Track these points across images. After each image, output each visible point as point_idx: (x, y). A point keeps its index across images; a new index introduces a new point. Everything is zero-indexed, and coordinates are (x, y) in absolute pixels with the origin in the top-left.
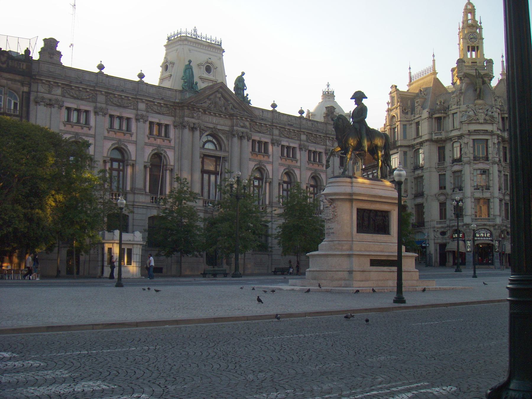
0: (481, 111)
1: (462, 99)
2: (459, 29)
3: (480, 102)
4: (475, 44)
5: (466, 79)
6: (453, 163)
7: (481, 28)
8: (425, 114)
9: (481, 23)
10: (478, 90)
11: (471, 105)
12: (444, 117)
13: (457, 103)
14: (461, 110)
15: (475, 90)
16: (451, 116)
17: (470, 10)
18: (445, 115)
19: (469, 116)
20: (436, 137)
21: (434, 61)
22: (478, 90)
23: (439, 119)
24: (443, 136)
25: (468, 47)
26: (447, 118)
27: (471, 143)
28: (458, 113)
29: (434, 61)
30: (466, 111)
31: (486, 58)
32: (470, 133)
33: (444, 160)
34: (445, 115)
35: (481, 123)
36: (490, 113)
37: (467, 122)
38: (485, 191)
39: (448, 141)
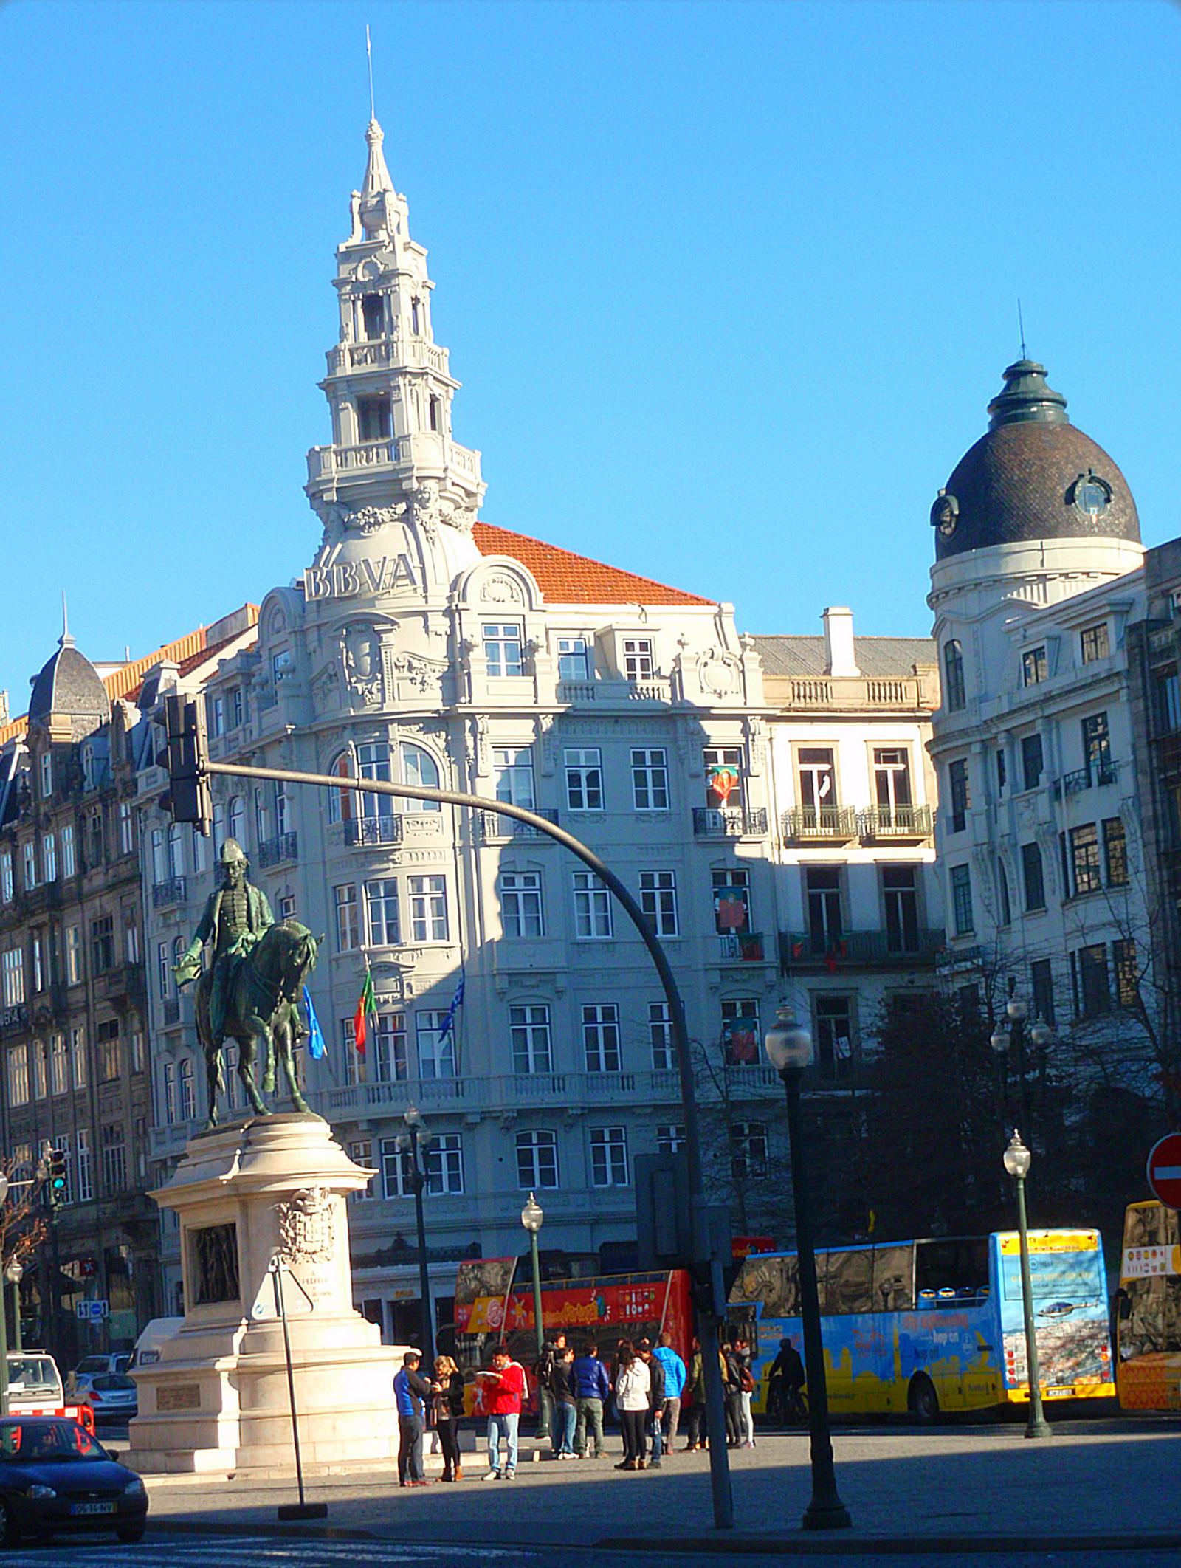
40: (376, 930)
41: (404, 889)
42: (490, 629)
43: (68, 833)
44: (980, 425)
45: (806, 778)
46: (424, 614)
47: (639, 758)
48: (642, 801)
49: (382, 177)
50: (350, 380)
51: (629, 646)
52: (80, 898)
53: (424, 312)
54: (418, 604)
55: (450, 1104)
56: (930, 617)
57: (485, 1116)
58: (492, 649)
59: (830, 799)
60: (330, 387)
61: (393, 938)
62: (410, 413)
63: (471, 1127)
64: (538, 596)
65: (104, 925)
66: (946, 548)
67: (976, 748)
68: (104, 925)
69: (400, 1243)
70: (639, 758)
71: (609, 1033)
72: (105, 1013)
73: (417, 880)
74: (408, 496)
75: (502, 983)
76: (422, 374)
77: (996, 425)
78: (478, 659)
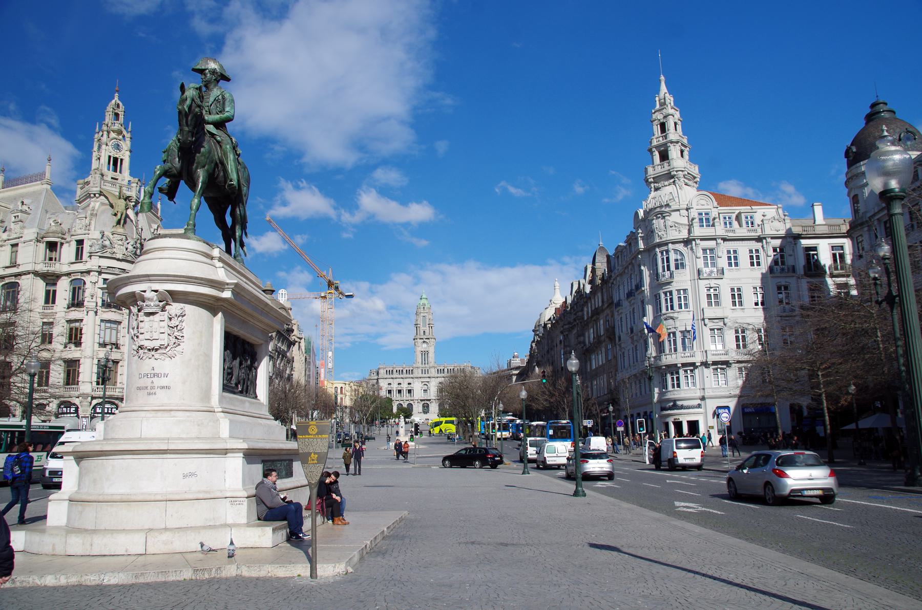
0: (120, 242)
1: (93, 222)
3: (120, 230)
6: (68, 308)
8: (30, 233)
12: (62, 244)
14: (90, 236)
16: (74, 244)
19: (104, 247)
20: (46, 269)
23: (52, 246)
24: (57, 268)
25: (110, 157)
26: (65, 246)
27: (101, 284)
33: (54, 302)
35: (118, 260)
37: (99, 254)
38: (114, 350)
39: (63, 278)
40: (667, 307)
41: (675, 294)
43: (600, 295)
46: (678, 210)
47: (751, 251)
48: (752, 264)
49: (663, 88)
50: (656, 147)
51: (747, 218)
52: (603, 311)
53: (679, 127)
54: (677, 207)
58: (701, 220)
61: (672, 308)
62: (674, 152)
63: (696, 367)
64: (716, 204)
67: (866, 229)
71: (744, 337)
73: (679, 291)
74: (673, 177)
76: (677, 142)
77: (866, 124)
78: (696, 223)
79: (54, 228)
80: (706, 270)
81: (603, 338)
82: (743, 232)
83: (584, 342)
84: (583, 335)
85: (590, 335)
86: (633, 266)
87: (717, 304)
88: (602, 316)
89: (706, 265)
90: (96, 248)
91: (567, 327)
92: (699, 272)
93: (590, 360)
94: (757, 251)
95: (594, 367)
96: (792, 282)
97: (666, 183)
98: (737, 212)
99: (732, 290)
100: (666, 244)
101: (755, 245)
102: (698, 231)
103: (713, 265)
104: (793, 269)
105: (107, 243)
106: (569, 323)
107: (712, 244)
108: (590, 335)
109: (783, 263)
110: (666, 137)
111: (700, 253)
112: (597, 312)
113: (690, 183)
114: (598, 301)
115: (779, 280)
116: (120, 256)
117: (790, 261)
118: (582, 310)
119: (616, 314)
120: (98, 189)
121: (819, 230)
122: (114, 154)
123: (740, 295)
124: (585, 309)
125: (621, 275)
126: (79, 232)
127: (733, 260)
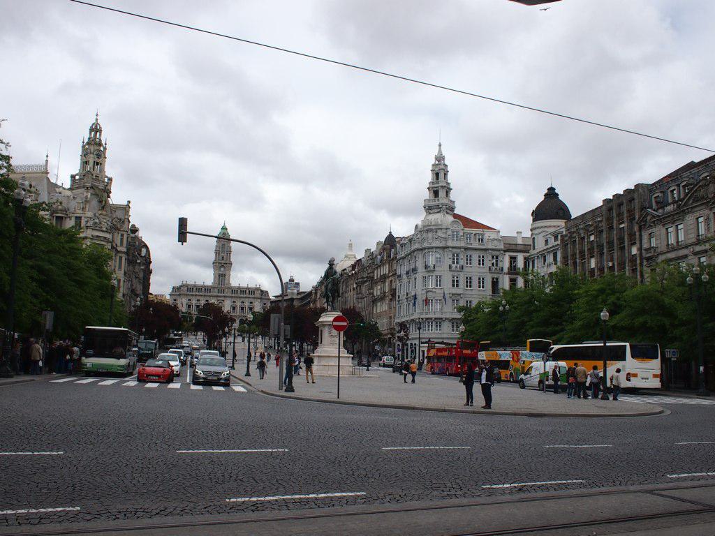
1: (87, 206)
2: (83, 142)
3: (104, 213)
4: (99, 161)
5: (92, 190)
7: (105, 149)
9: (106, 144)
10: (104, 202)
11: (97, 215)
13: (83, 209)
15: (101, 202)
16: (73, 219)
17: (96, 129)
18: (66, 216)
19: (96, 223)
21: (47, 161)
22: (104, 202)
28: (82, 218)
29: (47, 161)
30: (91, 218)
31: (106, 174)
32: (93, 238)
34: (66, 216)
36: (110, 224)
42: (453, 232)
43: (387, 266)
44: (542, 198)
45: (511, 262)
47: (480, 257)
48: (479, 264)
52: (389, 277)
55: (441, 316)
56: (530, 233)
57: (446, 319)
59: (515, 266)
60: (428, 188)
65: (391, 281)
66: (534, 220)
68: (391, 281)
69: (429, 340)
70: (480, 257)
72: (390, 297)
75: (451, 295)
79: (60, 207)
80: (454, 266)
81: (387, 294)
82: (476, 245)
83: (373, 293)
84: (373, 289)
85: (377, 291)
86: (411, 258)
87: (457, 286)
88: (388, 281)
89: (454, 263)
90: (90, 224)
91: (360, 280)
92: (450, 267)
93: (376, 305)
94: (483, 257)
95: (378, 311)
96: (500, 276)
97: (436, 211)
98: (474, 233)
99: (467, 278)
100: (432, 248)
101: (482, 254)
102: (450, 244)
103: (457, 263)
104: (502, 269)
105: (97, 221)
106: (362, 278)
107: (458, 251)
108: (377, 291)
109: (497, 265)
110: (438, 183)
111: (451, 256)
112: (384, 278)
113: (449, 212)
114: (385, 270)
115: (493, 275)
116: (105, 229)
117: (500, 264)
118: (373, 272)
119: (398, 281)
120: (90, 185)
121: (519, 248)
122: (97, 160)
123: (470, 282)
124: (376, 272)
125: (404, 258)
126: (78, 211)
127: (469, 260)
